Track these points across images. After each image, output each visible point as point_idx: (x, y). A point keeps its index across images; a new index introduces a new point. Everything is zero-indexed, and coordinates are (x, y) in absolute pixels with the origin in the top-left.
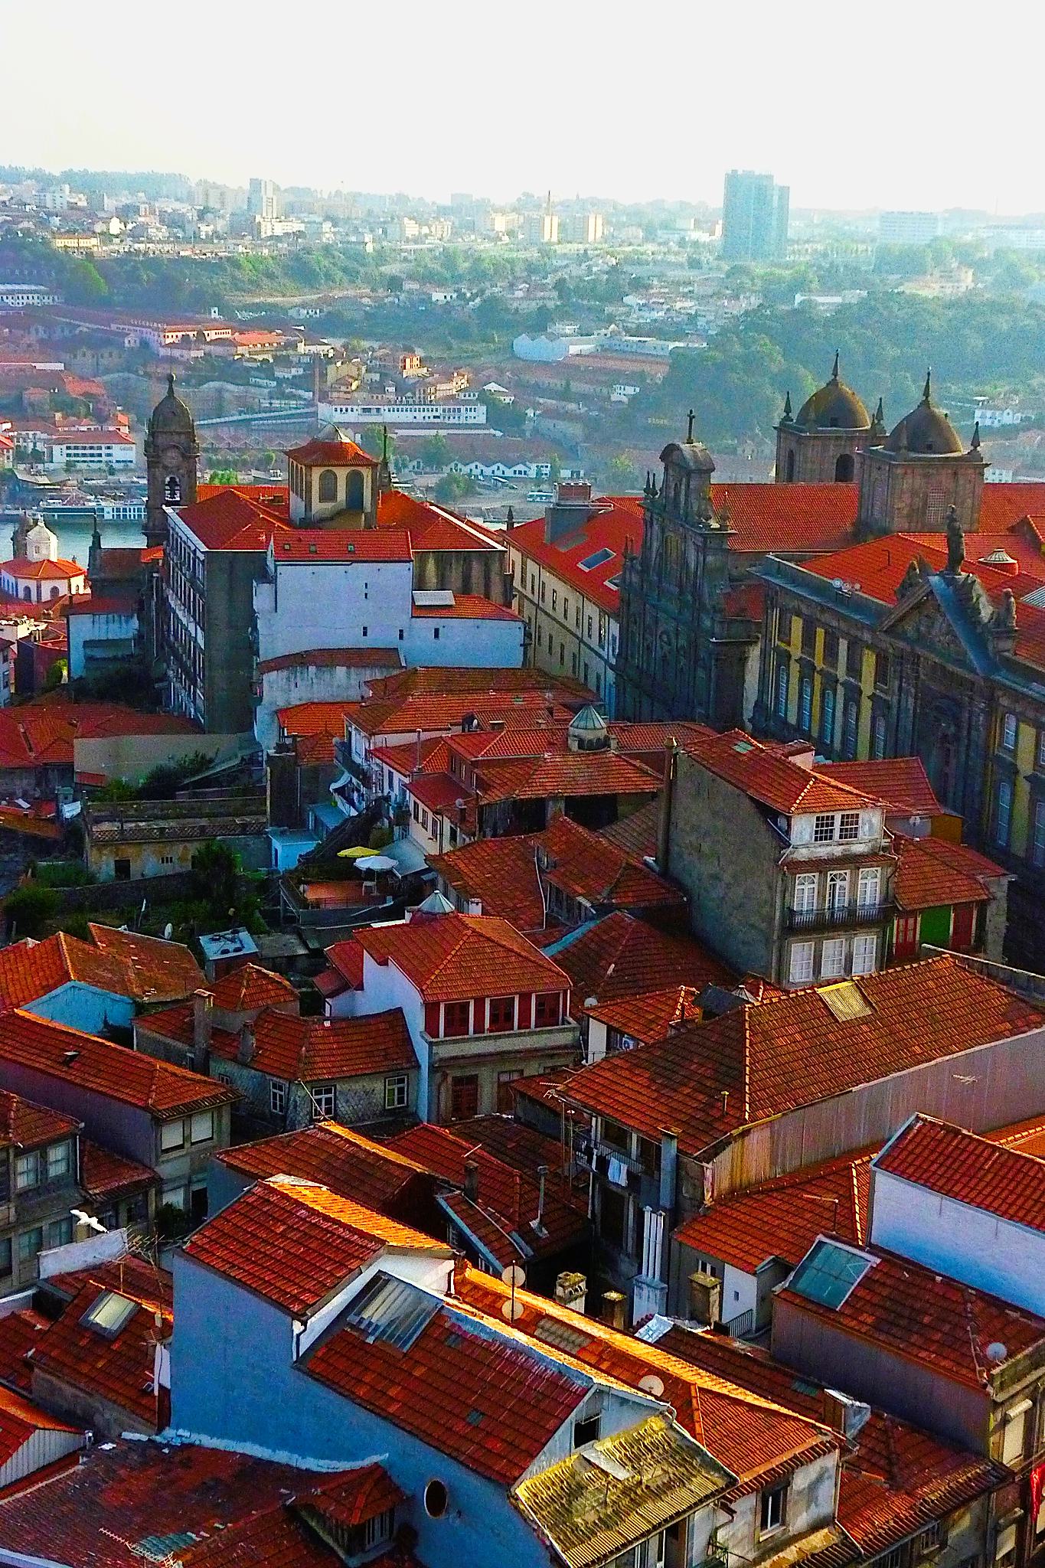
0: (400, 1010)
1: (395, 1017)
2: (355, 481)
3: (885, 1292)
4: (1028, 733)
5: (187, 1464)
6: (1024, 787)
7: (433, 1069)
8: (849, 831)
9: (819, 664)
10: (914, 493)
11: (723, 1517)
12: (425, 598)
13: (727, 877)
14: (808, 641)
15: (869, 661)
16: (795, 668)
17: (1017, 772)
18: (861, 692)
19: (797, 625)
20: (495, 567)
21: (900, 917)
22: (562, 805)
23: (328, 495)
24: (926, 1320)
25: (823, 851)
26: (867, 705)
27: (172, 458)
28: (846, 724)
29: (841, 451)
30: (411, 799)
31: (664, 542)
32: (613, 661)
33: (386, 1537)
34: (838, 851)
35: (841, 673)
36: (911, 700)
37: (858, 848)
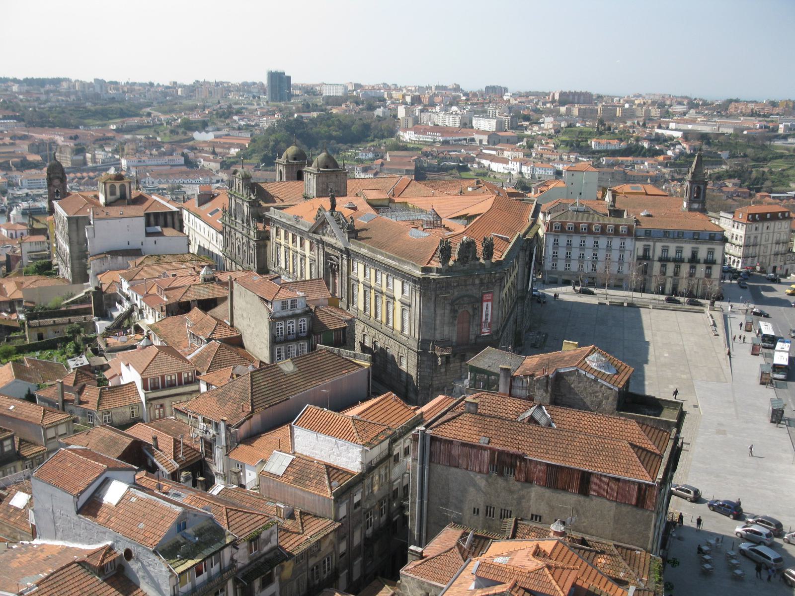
0: (134, 382)
1: (132, 384)
2: (123, 187)
3: (298, 468)
4: (361, 267)
5: (42, 551)
6: (361, 286)
7: (146, 403)
8: (294, 306)
9: (291, 245)
10: (323, 183)
11: (234, 550)
12: (151, 229)
13: (253, 325)
14: (286, 238)
15: (307, 244)
16: (283, 248)
17: (358, 281)
18: (305, 256)
19: (282, 232)
20: (176, 217)
21: (315, 335)
22: (196, 303)
23: (113, 193)
24: (312, 476)
25: (285, 314)
26: (308, 260)
27: (56, 182)
28: (301, 267)
29: (298, 169)
30: (144, 304)
31: (236, 203)
32: (221, 249)
33: (113, 569)
34: (290, 313)
35: (298, 249)
36: (322, 258)
37: (298, 311)
